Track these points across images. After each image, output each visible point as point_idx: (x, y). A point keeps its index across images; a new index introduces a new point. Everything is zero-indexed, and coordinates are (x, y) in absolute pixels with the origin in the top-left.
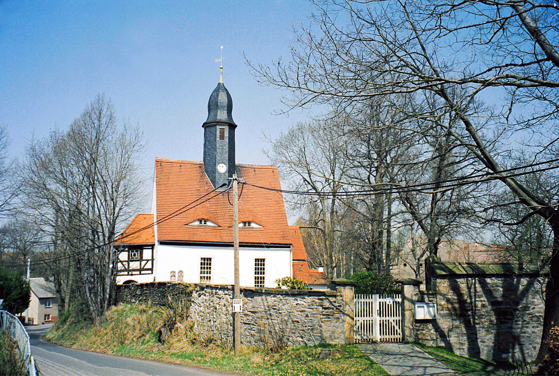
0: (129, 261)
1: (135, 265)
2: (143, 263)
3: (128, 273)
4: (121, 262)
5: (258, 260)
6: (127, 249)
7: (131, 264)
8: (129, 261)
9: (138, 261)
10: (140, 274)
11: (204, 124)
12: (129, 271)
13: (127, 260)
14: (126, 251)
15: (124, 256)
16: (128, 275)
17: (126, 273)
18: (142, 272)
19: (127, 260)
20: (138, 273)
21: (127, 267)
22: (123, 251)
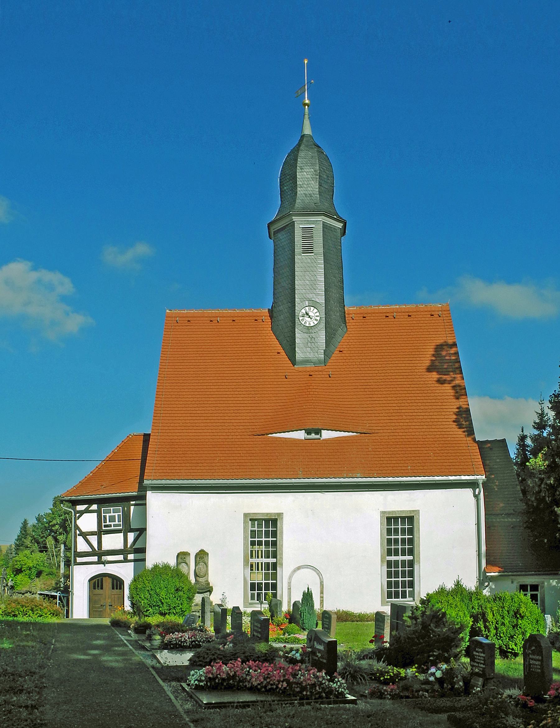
0: (99, 533)
4: (84, 535)
5: (396, 519)
6: (94, 507)
7: (106, 538)
8: (99, 533)
9: (119, 531)
12: (100, 554)
13: (95, 528)
15: (88, 522)
16: (100, 562)
17: (95, 559)
19: (95, 528)
20: (121, 557)
21: (95, 546)
22: (87, 511)
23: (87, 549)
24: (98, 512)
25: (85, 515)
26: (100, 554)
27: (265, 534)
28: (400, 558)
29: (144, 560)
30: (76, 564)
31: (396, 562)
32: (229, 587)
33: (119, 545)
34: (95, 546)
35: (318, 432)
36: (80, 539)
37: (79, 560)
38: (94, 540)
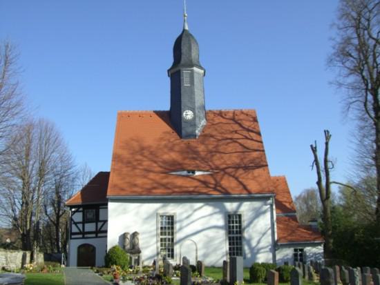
0: (83, 223)
1: (90, 227)
2: (100, 224)
3: (83, 236)
6: (81, 209)
7: (86, 225)
8: (83, 223)
10: (97, 237)
11: (168, 71)
12: (83, 234)
13: (81, 220)
14: (80, 211)
16: (83, 238)
17: (81, 236)
18: (99, 235)
20: (94, 235)
21: (82, 230)
23: (77, 231)
24: (83, 211)
25: (76, 214)
26: (83, 234)
27: (169, 225)
28: (235, 235)
29: (106, 237)
30: (71, 238)
31: (233, 237)
32: (149, 249)
33: (94, 229)
34: (82, 230)
35: (193, 172)
36: (74, 226)
37: (73, 237)
38: (80, 226)
